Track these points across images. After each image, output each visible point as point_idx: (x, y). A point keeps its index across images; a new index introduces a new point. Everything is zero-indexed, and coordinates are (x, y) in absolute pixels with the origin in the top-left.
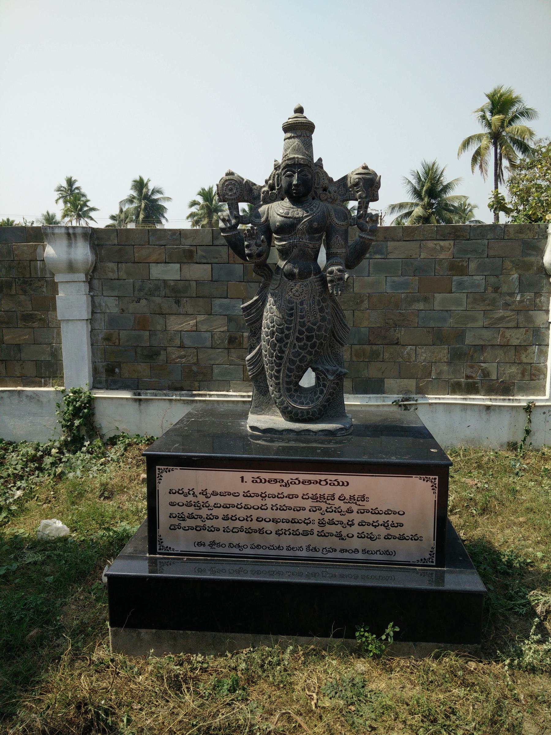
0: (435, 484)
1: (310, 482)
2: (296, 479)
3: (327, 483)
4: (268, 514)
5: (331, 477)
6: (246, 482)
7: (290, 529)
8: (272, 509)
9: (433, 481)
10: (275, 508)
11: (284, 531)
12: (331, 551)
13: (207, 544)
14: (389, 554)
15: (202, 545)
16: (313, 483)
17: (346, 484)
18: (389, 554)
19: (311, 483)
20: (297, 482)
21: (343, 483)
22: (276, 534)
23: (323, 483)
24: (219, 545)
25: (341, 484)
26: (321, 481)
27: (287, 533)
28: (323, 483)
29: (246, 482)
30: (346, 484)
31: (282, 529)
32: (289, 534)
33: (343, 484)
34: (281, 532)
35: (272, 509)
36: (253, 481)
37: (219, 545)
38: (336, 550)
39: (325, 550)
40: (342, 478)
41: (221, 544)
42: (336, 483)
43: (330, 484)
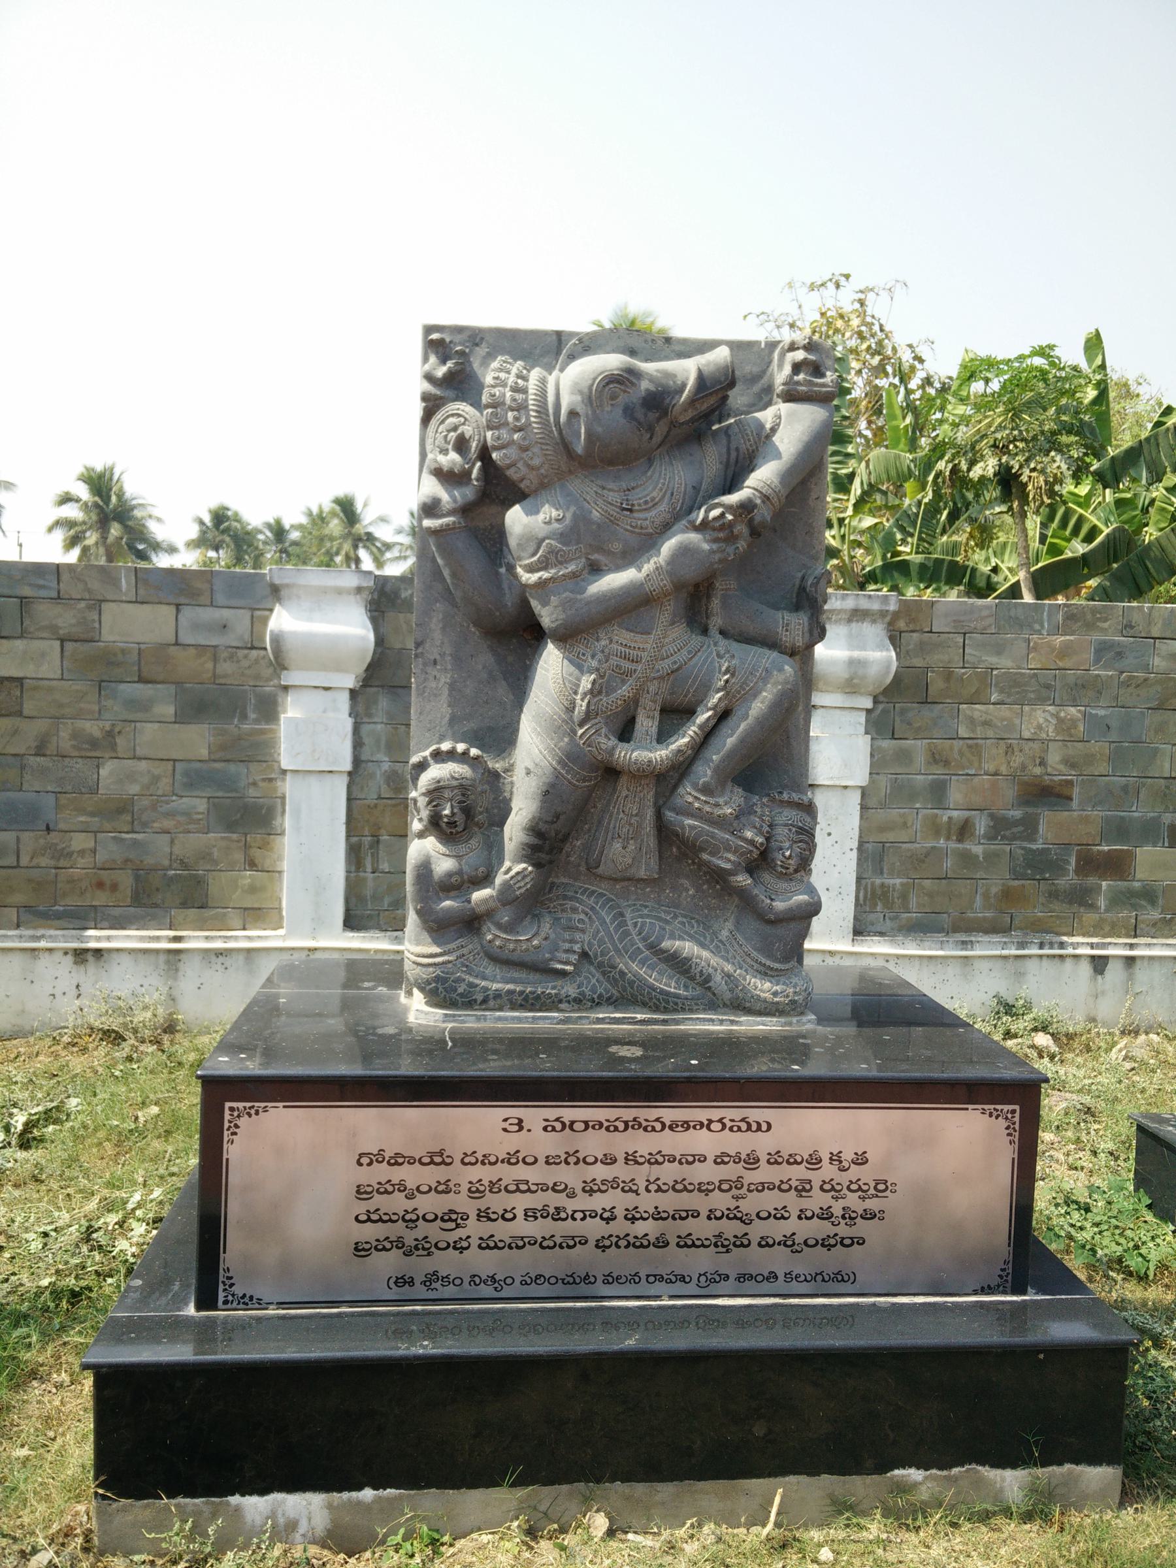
0: (1014, 1123)
1: (686, 1126)
2: (557, 1120)
3: (724, 1126)
4: (647, 1202)
5: (732, 1113)
6: (529, 1131)
7: (628, 1235)
8: (648, 1191)
9: (1009, 1116)
10: (653, 1187)
11: (614, 1240)
12: (718, 1279)
13: (417, 1282)
14: (843, 1280)
15: (405, 1282)
16: (694, 1127)
17: (764, 1127)
18: (843, 1280)
19: (688, 1129)
20: (658, 1126)
21: (759, 1124)
22: (597, 1246)
23: (716, 1126)
25: (754, 1127)
26: (710, 1121)
27: (623, 1243)
28: (716, 1126)
29: (529, 1131)
30: (764, 1127)
31: (611, 1236)
32: (627, 1247)
33: (759, 1128)
34: (607, 1243)
35: (648, 1191)
36: (545, 1129)
38: (728, 1277)
39: (703, 1279)
40: (757, 1114)
41: (451, 1278)
43: (731, 1129)
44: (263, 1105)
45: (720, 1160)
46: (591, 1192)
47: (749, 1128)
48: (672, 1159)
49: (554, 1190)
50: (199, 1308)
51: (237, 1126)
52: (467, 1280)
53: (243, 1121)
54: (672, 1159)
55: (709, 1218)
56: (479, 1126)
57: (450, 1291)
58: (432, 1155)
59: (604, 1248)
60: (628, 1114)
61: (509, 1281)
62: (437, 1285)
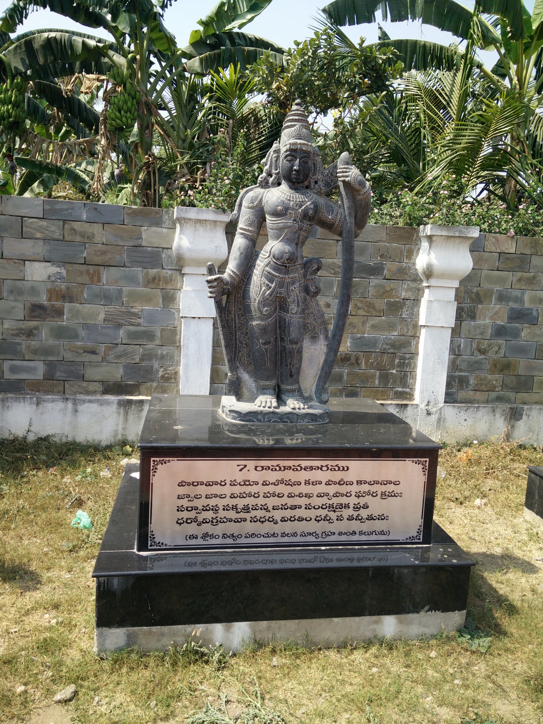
17: (346, 469)
21: (343, 468)
23: (325, 468)
24: (212, 536)
25: (341, 469)
26: (322, 466)
28: (325, 468)
30: (346, 469)
37: (212, 536)
40: (342, 463)
42: (337, 468)
43: (331, 470)
44: (168, 459)
45: (328, 483)
46: (359, 497)
47: (339, 469)
48: (202, 483)
49: (278, 496)
50: (139, 550)
51: (156, 469)
52: (221, 536)
53: (159, 467)
54: (202, 483)
55: (306, 508)
56: (226, 469)
57: (214, 541)
58: (245, 481)
59: (318, 521)
60: (330, 463)
61: (240, 536)
62: (208, 538)
